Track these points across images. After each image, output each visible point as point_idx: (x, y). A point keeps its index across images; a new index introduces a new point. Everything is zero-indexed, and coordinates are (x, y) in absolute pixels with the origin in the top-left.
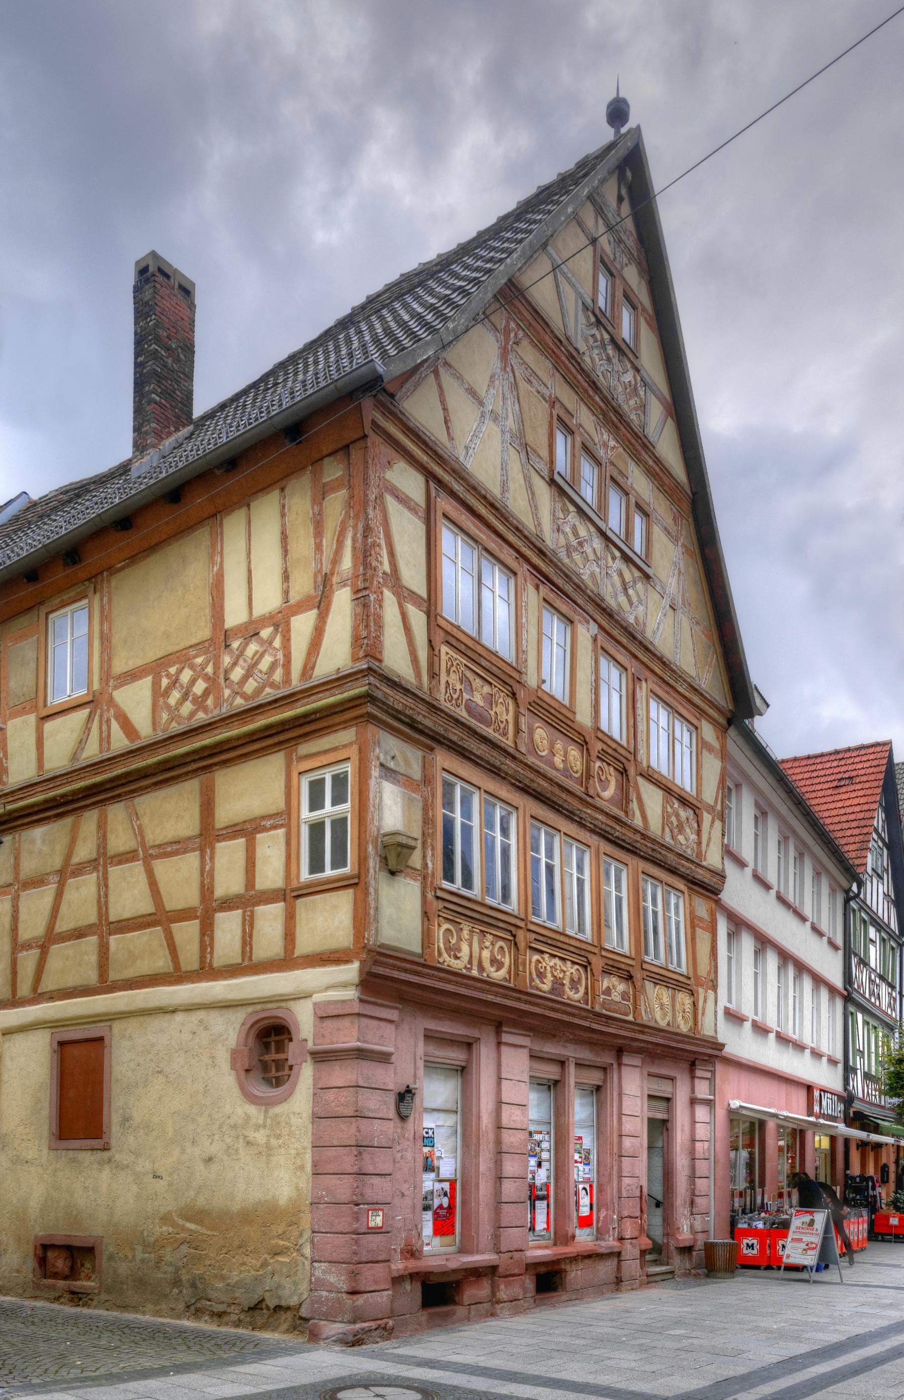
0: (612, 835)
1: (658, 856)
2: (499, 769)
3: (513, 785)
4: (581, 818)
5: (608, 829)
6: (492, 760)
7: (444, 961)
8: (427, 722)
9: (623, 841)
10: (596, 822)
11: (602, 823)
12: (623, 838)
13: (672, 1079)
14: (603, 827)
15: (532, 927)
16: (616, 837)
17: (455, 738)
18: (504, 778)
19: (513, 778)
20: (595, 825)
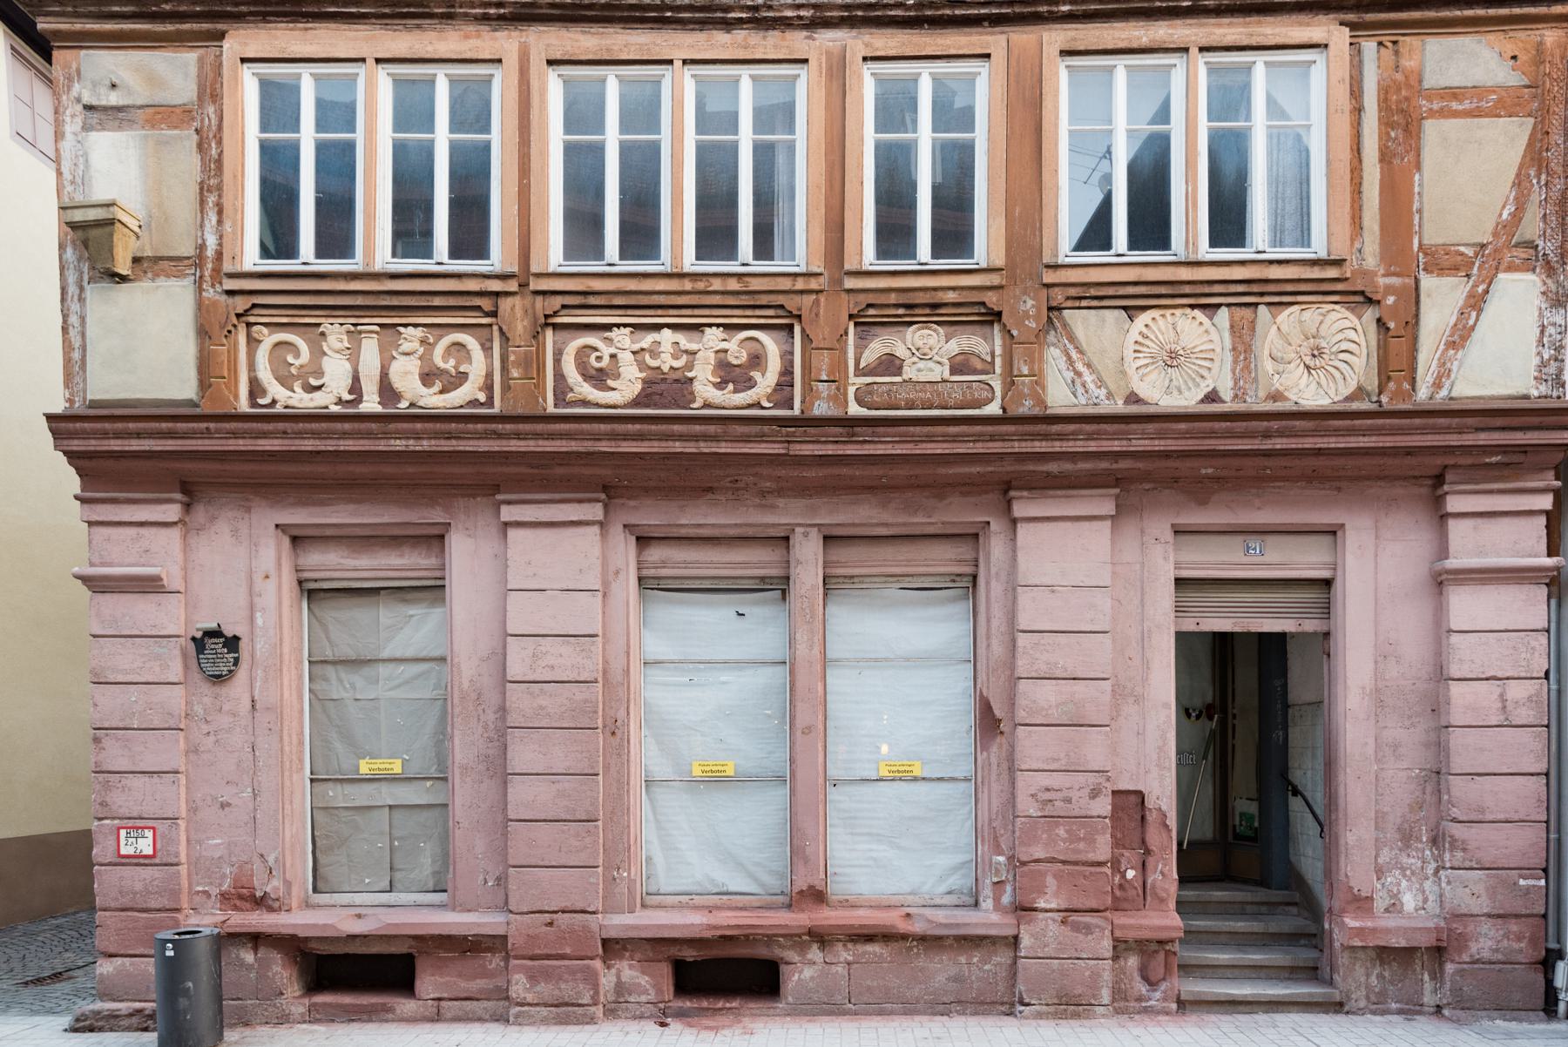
7: (274, 402)
13: (1332, 532)
15: (545, 285)
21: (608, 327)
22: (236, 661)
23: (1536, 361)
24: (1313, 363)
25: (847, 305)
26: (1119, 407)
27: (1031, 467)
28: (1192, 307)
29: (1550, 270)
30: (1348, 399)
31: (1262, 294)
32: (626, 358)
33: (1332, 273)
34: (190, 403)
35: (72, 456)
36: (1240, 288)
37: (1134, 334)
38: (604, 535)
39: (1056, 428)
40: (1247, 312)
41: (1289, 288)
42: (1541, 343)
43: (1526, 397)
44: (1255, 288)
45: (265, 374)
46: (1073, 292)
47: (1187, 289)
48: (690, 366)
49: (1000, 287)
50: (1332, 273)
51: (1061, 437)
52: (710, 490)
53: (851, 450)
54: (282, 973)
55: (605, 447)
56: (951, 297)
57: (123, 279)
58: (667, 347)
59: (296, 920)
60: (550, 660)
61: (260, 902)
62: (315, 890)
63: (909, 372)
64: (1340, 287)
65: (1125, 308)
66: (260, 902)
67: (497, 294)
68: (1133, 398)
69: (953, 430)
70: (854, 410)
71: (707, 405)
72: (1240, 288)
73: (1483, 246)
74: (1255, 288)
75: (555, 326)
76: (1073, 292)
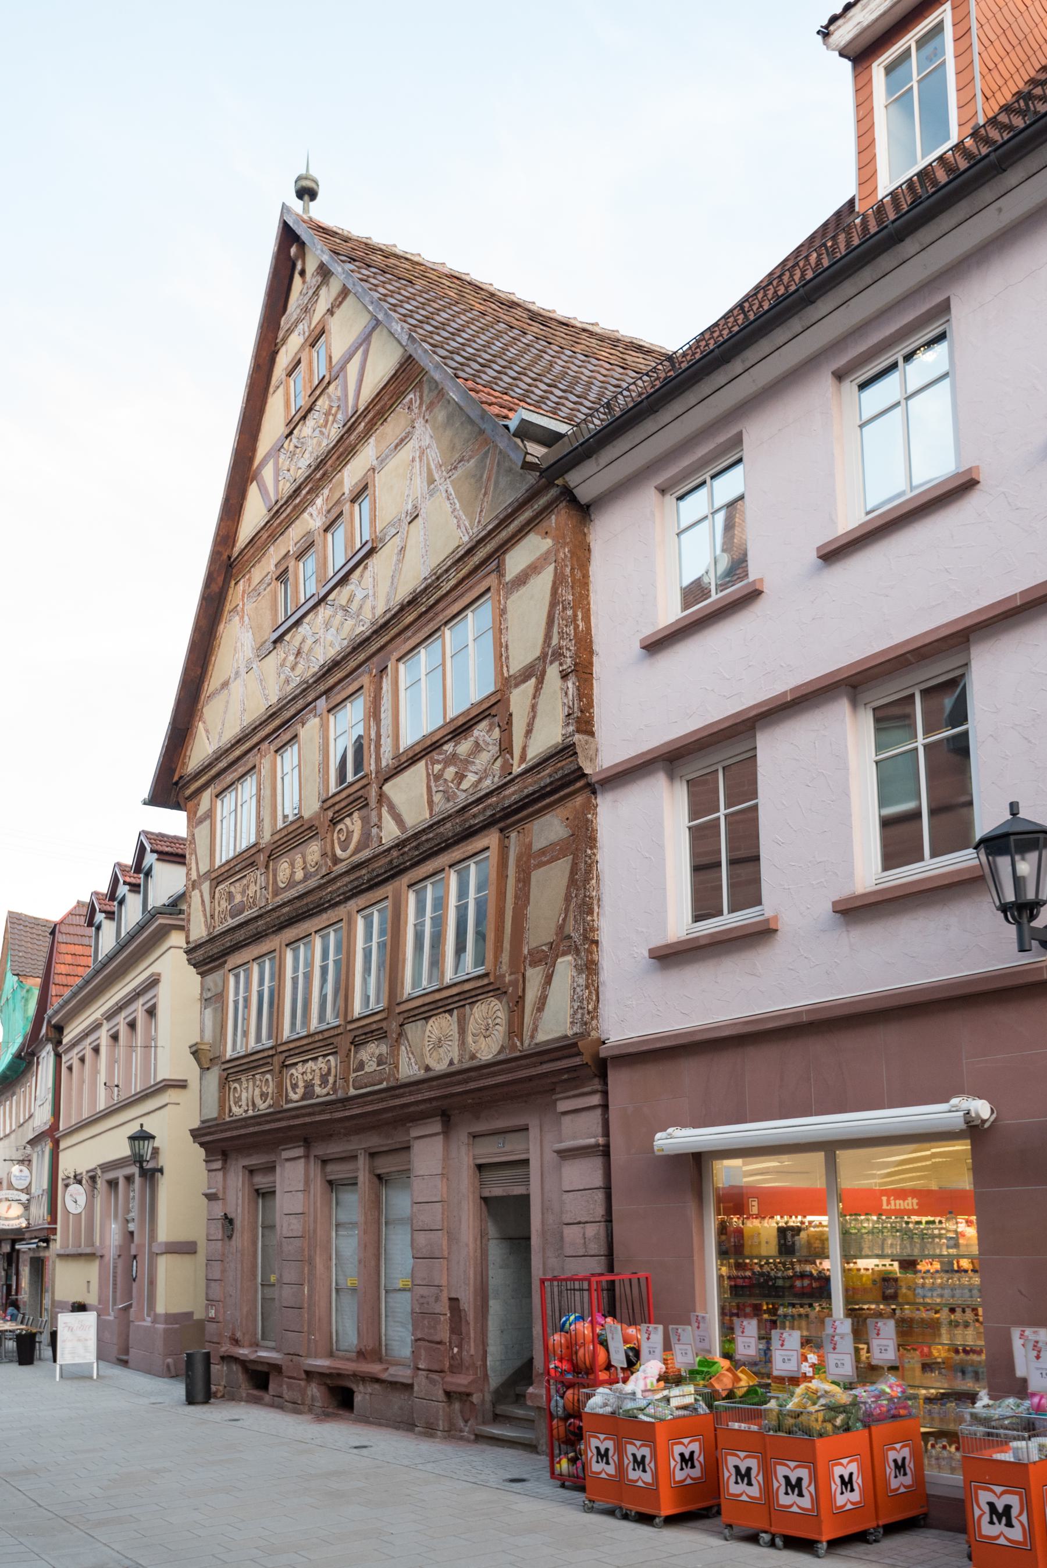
0: (363, 884)
1: (428, 846)
2: (259, 933)
3: (273, 932)
4: (329, 901)
5: (356, 883)
6: (251, 933)
8: (216, 951)
9: (378, 876)
10: (341, 891)
11: (346, 885)
12: (375, 873)
14: (350, 887)
16: (369, 881)
17: (229, 944)
18: (266, 935)
19: (269, 929)
20: (343, 893)
21: (296, 1064)
22: (233, 1230)
23: (570, 1012)
24: (483, 1035)
25: (350, 1037)
26: (421, 1074)
27: (406, 1111)
28: (445, 1012)
29: (577, 951)
30: (499, 1053)
31: (466, 999)
32: (300, 1076)
33: (486, 981)
34: (215, 1119)
35: (202, 1145)
36: (456, 998)
37: (428, 1033)
38: (307, 1163)
39: (397, 1092)
40: (461, 1010)
41: (474, 993)
42: (573, 1000)
43: (566, 1037)
44: (462, 997)
45: (232, 1103)
46: (406, 1015)
47: (440, 1004)
48: (313, 1079)
49: (385, 1019)
50: (486, 981)
51: (401, 1096)
52: (331, 1135)
53: (347, 1114)
54: (240, 1376)
55: (292, 1123)
56: (374, 1027)
57: (208, 1069)
58: (309, 1070)
59: (243, 1352)
60: (292, 1227)
61: (236, 1342)
62: (263, 1339)
63: (367, 1069)
64: (491, 988)
65: (424, 1018)
66: (236, 1342)
67: (273, 1056)
68: (428, 1069)
69: (369, 1098)
70: (352, 1092)
71: (318, 1096)
72: (456, 998)
73: (552, 943)
74: (462, 997)
75: (287, 1066)
76: (406, 1015)
